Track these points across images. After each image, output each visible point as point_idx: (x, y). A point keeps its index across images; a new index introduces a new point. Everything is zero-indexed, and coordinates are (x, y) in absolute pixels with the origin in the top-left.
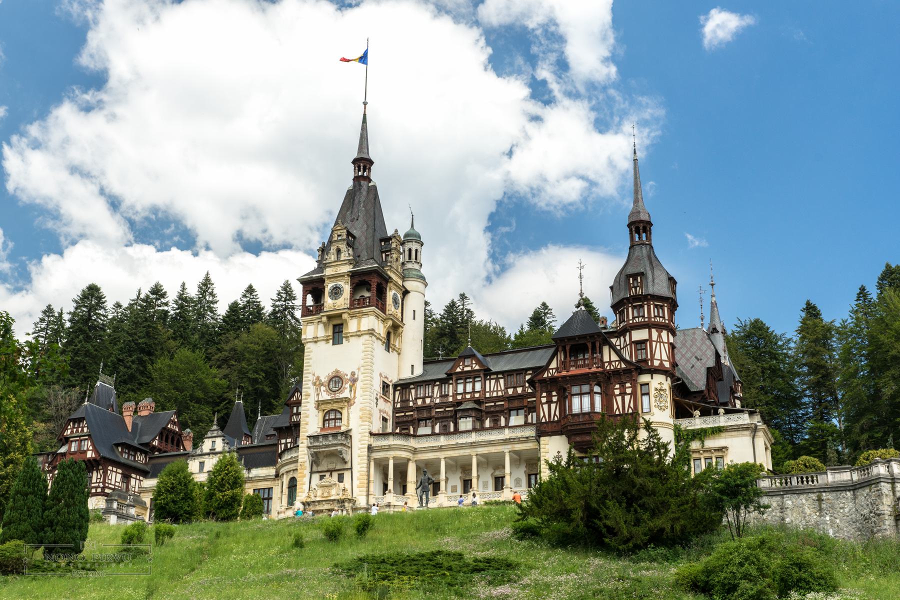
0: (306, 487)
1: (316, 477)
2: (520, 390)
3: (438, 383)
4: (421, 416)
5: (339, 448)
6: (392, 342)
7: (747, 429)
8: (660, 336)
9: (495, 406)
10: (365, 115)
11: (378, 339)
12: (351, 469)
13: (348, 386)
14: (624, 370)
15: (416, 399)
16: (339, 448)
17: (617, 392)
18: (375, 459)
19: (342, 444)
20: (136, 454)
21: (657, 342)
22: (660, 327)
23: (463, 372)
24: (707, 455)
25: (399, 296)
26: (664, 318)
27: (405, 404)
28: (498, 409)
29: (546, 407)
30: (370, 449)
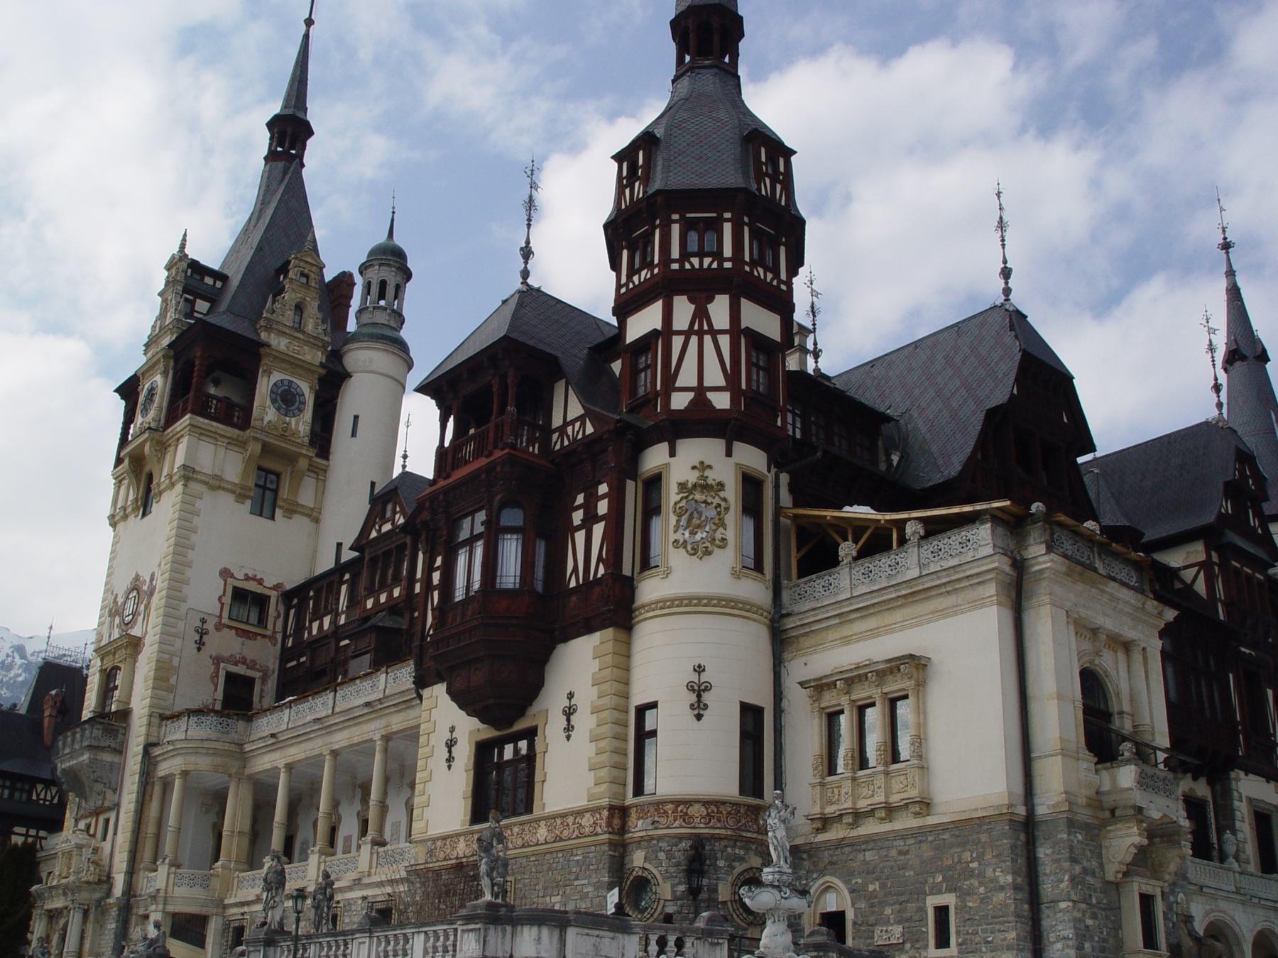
3: (347, 576)
5: (85, 757)
6: (284, 492)
7: (977, 580)
8: (701, 314)
10: (306, 36)
11: (213, 488)
13: (142, 607)
14: (589, 442)
17: (578, 517)
19: (90, 747)
20: (33, 786)
21: (688, 334)
22: (700, 288)
23: (382, 537)
24: (860, 694)
25: (306, 389)
26: (718, 255)
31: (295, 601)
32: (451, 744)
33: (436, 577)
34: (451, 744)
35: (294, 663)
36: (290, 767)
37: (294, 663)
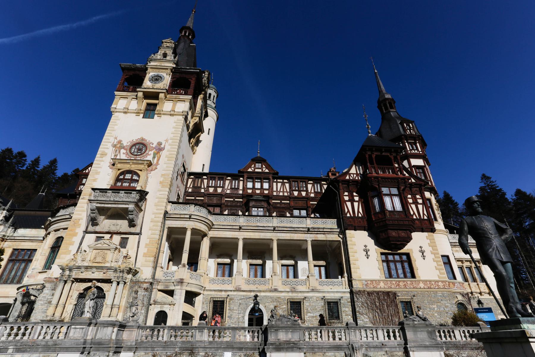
0: (73, 249)
1: (90, 238)
2: (304, 194)
3: (229, 178)
4: (211, 202)
9: (281, 203)
12: (139, 234)
15: (208, 187)
16: (131, 207)
18: (169, 228)
23: (254, 172)
27: (196, 190)
28: (283, 206)
29: (349, 204)
30: (166, 215)
31: (192, 177)
32: (367, 251)
33: (346, 198)
34: (367, 251)
35: (193, 198)
36: (244, 239)
37: (193, 198)
